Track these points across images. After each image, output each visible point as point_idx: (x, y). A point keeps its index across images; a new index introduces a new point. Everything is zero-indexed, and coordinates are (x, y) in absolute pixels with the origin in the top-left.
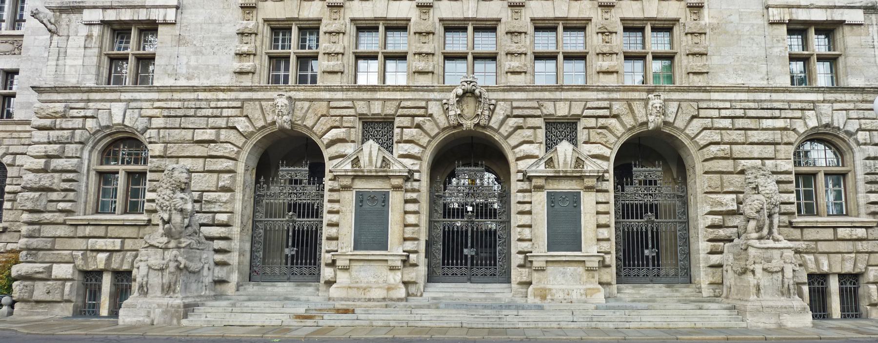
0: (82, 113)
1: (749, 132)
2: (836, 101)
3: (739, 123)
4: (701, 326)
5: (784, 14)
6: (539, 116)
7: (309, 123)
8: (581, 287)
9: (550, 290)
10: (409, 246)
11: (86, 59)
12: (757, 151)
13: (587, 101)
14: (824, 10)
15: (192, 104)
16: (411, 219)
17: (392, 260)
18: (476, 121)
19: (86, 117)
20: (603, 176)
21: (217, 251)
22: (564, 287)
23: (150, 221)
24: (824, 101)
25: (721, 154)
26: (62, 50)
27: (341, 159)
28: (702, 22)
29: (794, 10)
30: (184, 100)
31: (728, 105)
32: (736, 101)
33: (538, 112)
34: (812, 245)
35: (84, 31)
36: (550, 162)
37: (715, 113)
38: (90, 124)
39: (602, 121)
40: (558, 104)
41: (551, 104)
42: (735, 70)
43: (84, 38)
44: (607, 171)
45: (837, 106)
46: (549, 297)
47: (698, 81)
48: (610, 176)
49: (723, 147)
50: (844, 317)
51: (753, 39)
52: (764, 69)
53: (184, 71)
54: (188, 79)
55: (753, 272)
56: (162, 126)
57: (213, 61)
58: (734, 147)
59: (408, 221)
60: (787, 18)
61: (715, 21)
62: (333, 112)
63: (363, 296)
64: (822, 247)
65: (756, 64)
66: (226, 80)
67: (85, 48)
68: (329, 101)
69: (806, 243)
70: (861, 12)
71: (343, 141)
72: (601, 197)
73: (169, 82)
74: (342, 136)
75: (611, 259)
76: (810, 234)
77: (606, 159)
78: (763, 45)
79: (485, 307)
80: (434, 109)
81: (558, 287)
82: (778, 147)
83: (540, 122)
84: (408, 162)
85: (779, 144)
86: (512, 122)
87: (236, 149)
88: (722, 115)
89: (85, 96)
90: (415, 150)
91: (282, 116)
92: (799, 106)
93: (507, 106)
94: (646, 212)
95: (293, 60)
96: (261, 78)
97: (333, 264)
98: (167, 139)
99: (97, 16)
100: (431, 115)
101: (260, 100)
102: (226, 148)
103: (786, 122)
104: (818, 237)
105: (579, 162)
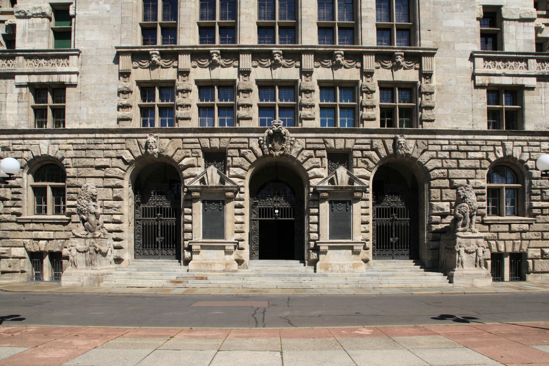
0: (21, 147)
1: (460, 161)
2: (516, 140)
3: (454, 155)
4: (425, 286)
5: (485, 79)
6: (323, 149)
7: (170, 154)
8: (350, 262)
9: (331, 264)
10: (238, 236)
11: (20, 109)
12: (464, 173)
13: (355, 139)
14: (511, 78)
15: (92, 141)
16: (239, 219)
17: (228, 246)
18: (282, 152)
19: (23, 150)
20: (366, 190)
21: (116, 240)
22: (339, 262)
23: (70, 220)
24: (508, 140)
25: (442, 175)
26: (3, 103)
27: (192, 179)
28: (432, 85)
29: (492, 77)
30: (87, 138)
31: (447, 142)
32: (452, 140)
33: (323, 146)
34: (495, 235)
35: (17, 90)
36: (332, 181)
37: (438, 148)
38: (26, 154)
39: (366, 153)
40: (337, 140)
41: (332, 141)
42: (452, 118)
43: (17, 95)
44: (368, 187)
45: (516, 143)
46: (330, 269)
47: (427, 126)
48: (370, 190)
49: (443, 171)
50: (511, 280)
51: (464, 97)
52: (470, 117)
53: (85, 118)
54: (88, 123)
55: (459, 252)
56: (74, 156)
57: (104, 110)
58: (450, 171)
59: (238, 219)
60: (487, 82)
61: (440, 84)
62: (186, 146)
63: (210, 269)
64: (502, 236)
65: (465, 114)
66: (113, 125)
67: (18, 102)
68: (182, 138)
69: (492, 233)
70: (535, 79)
71: (192, 166)
72: (362, 203)
73: (76, 126)
74: (192, 163)
75: (370, 244)
76: (494, 228)
77: (368, 178)
78: (471, 101)
79: (290, 275)
80: (254, 144)
81: (335, 262)
82: (478, 171)
83: (325, 153)
84: (235, 180)
85: (478, 169)
86: (306, 153)
87: (123, 172)
88: (443, 149)
89: (21, 136)
90: (240, 172)
91: (153, 149)
92: (493, 143)
93: (302, 142)
94: (392, 213)
95: (157, 109)
96: (137, 123)
97: (189, 249)
98: (77, 165)
99: (24, 79)
100: (251, 148)
101: (137, 138)
102: (116, 171)
103: (483, 154)
104: (499, 229)
105: (351, 181)
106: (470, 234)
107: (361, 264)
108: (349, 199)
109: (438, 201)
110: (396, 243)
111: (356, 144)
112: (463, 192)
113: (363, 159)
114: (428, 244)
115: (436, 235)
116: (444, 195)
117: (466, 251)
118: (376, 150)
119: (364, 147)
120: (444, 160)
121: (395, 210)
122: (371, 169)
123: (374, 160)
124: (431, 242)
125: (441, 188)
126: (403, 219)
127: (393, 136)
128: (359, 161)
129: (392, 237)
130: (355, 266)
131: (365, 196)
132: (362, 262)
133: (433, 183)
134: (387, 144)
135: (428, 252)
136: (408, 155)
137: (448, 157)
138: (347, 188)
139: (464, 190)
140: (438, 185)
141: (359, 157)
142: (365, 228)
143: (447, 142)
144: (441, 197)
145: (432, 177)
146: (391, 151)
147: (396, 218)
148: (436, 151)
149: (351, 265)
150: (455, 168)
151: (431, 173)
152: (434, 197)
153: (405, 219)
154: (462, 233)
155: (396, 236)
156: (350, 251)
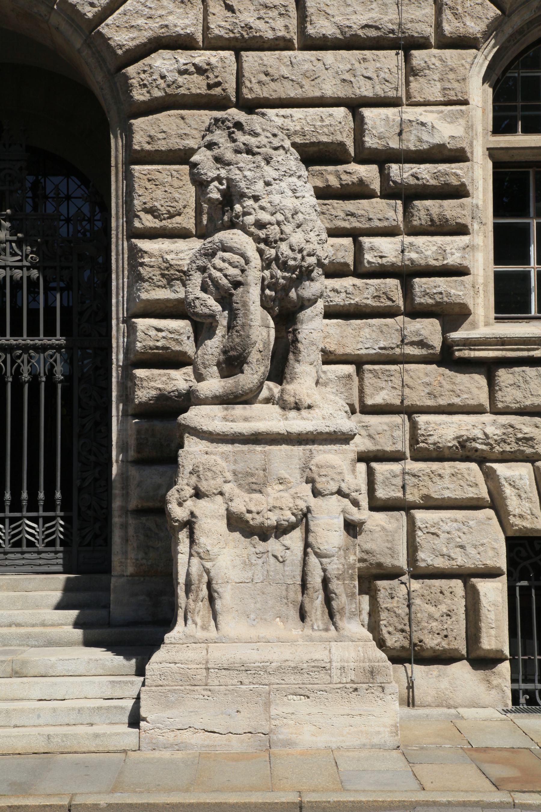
25: (196, 85)
49: (201, 57)
58: (251, 58)
82: (419, 56)
85: (422, 44)
106: (265, 418)
112: (218, 160)
117: (236, 523)
126: (25, 340)
133: (145, 130)
139: (226, 150)
145: (139, 95)
150: (281, 44)
151: (131, 70)
152: (152, 211)
153: (42, 340)
154: (217, 410)
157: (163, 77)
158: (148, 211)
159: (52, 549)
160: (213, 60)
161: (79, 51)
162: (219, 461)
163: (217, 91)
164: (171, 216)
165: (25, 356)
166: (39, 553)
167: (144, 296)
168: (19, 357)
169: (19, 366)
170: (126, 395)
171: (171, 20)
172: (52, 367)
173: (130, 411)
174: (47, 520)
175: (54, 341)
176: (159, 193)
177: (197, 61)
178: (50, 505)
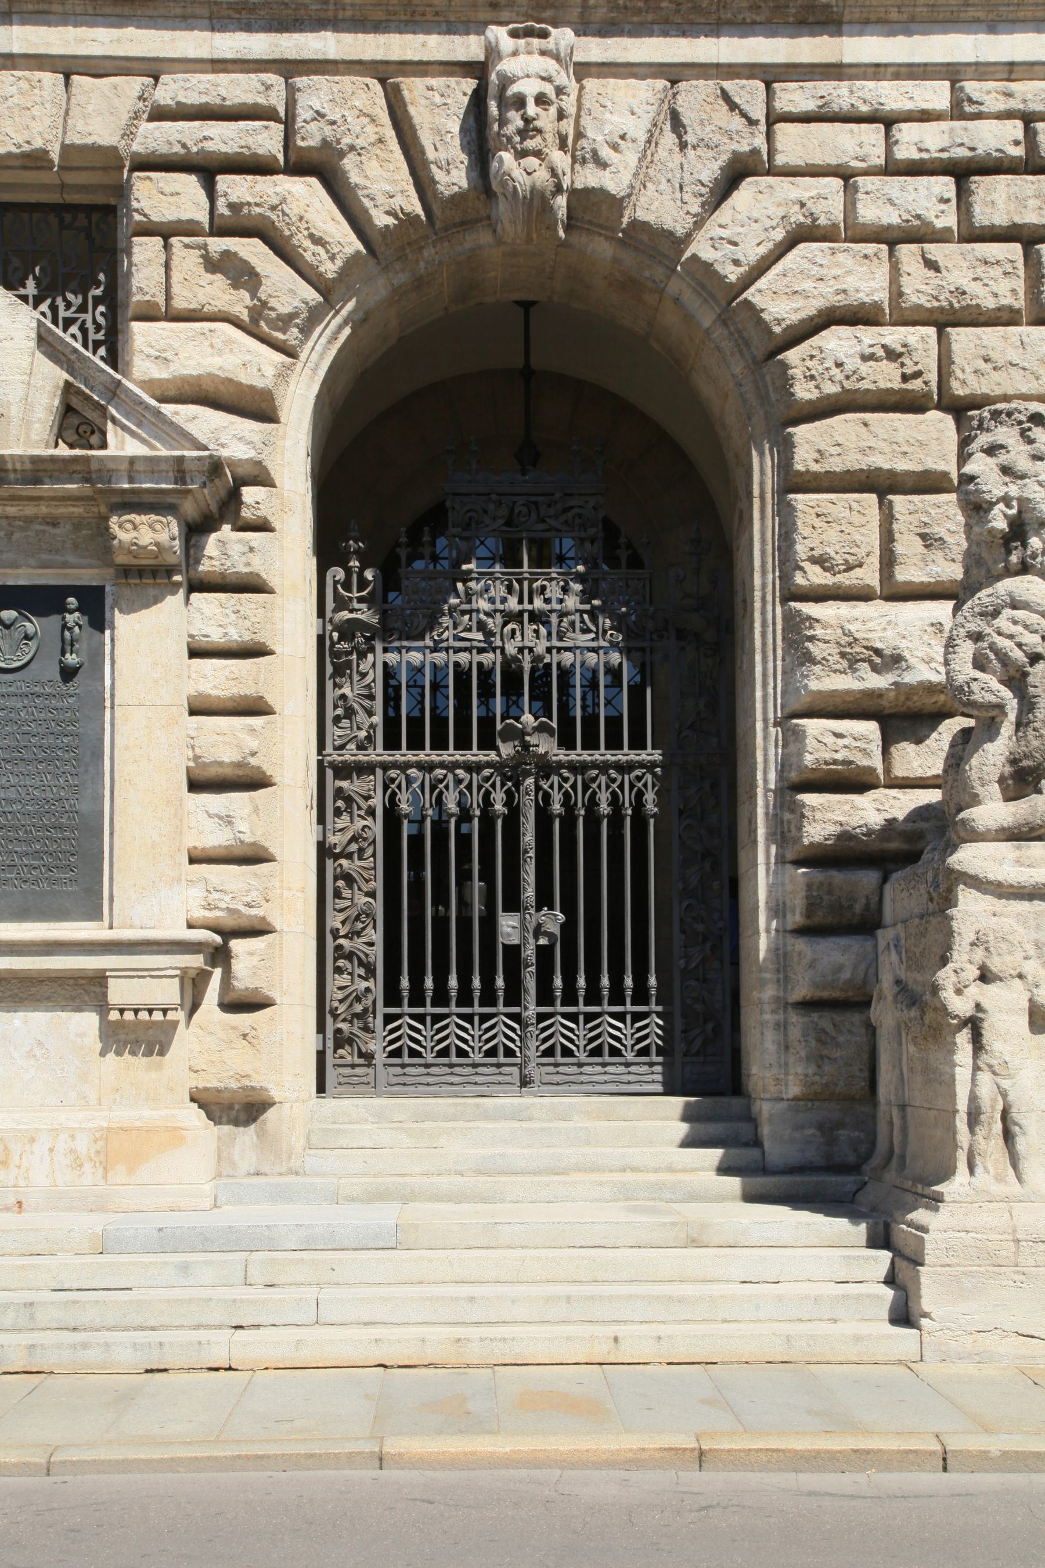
13: (153, 69)
25: (886, 377)
32: (982, 70)
37: (863, 143)
39: (234, 188)
44: (262, 478)
48: (289, 501)
49: (893, 336)
58: (962, 338)
72: (214, 616)
88: (903, 153)
107: (175, 1135)
108: (87, 576)
109: (863, 595)
110: (544, 954)
111: (159, 114)
112: (1006, 470)
113: (217, 245)
114: (781, 957)
115: (837, 877)
116: (907, 545)
118: (322, 166)
119: (223, 138)
120: (907, 252)
121: (544, 684)
122: (285, 321)
123: (311, 253)
124: (801, 945)
125: (882, 484)
126: (602, 755)
127: (468, 47)
128: (186, 258)
129: (513, 904)
130: (119, 1150)
131: (224, 549)
132: (196, 1116)
133: (814, 444)
134: (419, 114)
135: (782, 1027)
136: (593, 208)
137: (949, 220)
138: (39, 470)
139: (1018, 455)
140: (854, 461)
141: (188, 229)
142: (228, 820)
143: (936, 95)
144: (888, 560)
145: (804, 392)
146: (453, 176)
147: (546, 746)
148: (846, 175)
149: (83, 1145)
151: (792, 356)
152: (820, 561)
153: (626, 755)
154: (1006, 848)
155: (544, 900)
156: (90, 1021)
157: (839, 365)
158: (814, 561)
159: (550, 1060)
160: (912, 340)
161: (707, 332)
162: (1016, 927)
163: (916, 385)
164: (849, 568)
165: (603, 779)
166: (627, 1065)
167: (814, 685)
168: (594, 780)
169: (594, 793)
170: (784, 831)
171: (850, 282)
172: (640, 794)
173: (790, 855)
174: (637, 1017)
175: (644, 756)
176: (832, 534)
177: (888, 340)
178: (641, 995)
